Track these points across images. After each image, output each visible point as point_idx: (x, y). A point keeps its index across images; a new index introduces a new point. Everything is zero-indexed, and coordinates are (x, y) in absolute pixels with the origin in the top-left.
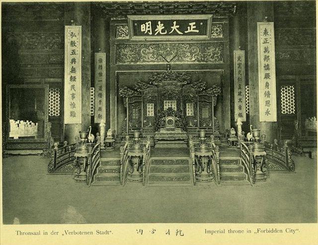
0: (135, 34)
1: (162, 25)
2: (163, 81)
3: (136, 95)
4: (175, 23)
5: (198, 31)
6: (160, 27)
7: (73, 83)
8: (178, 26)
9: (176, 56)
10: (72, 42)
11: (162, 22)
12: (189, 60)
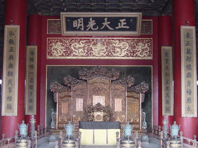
1: (94, 21)
4: (106, 19)
5: (128, 27)
6: (92, 24)
7: (10, 78)
8: (109, 23)
10: (10, 40)
11: (94, 18)
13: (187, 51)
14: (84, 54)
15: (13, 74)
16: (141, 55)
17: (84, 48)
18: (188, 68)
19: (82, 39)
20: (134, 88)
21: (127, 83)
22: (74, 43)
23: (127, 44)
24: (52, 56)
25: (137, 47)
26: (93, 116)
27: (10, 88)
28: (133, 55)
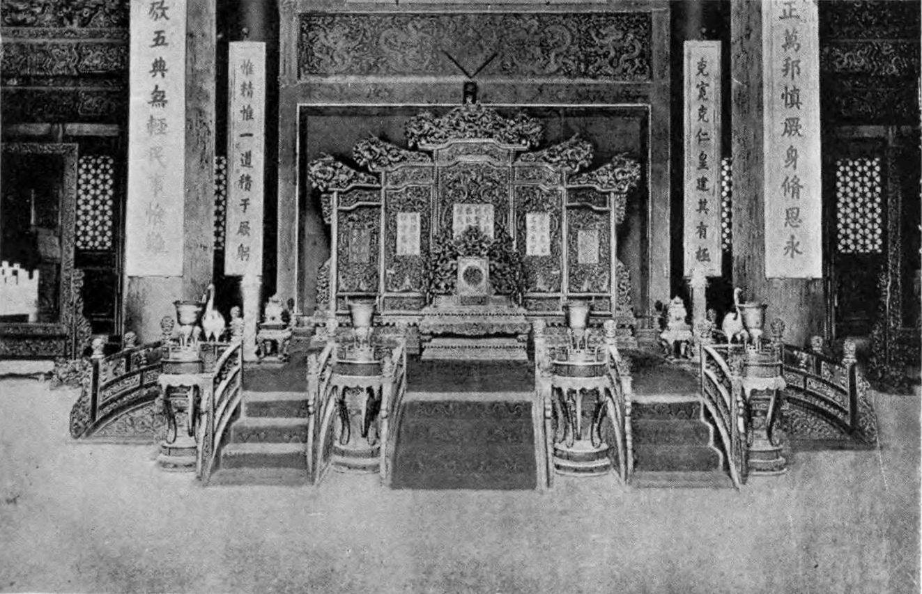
2: (451, 140)
3: (362, 184)
9: (496, 55)
18: (789, 101)
20: (592, 176)
21: (568, 161)
26: (455, 272)
28: (587, 68)
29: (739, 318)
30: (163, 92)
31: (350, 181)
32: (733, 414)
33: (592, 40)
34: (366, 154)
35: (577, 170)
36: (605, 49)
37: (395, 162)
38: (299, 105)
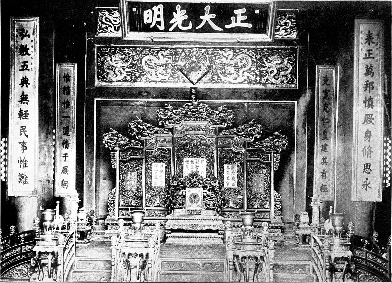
0: (133, 28)
2: (182, 122)
3: (133, 146)
7: (23, 122)
12: (233, 81)
13: (365, 69)
14: (166, 78)
15: (28, 114)
16: (275, 79)
17: (166, 66)
19: (163, 48)
20: (262, 143)
22: (146, 55)
23: (250, 59)
24: (105, 81)
25: (267, 64)
26: (184, 196)
27: (23, 142)
28: (260, 80)
29: (331, 221)
30: (27, 95)
31: (126, 145)
32: (324, 268)
33: (263, 63)
34: (135, 129)
35: (253, 139)
36: (271, 69)
37: (151, 134)
38: (95, 99)
